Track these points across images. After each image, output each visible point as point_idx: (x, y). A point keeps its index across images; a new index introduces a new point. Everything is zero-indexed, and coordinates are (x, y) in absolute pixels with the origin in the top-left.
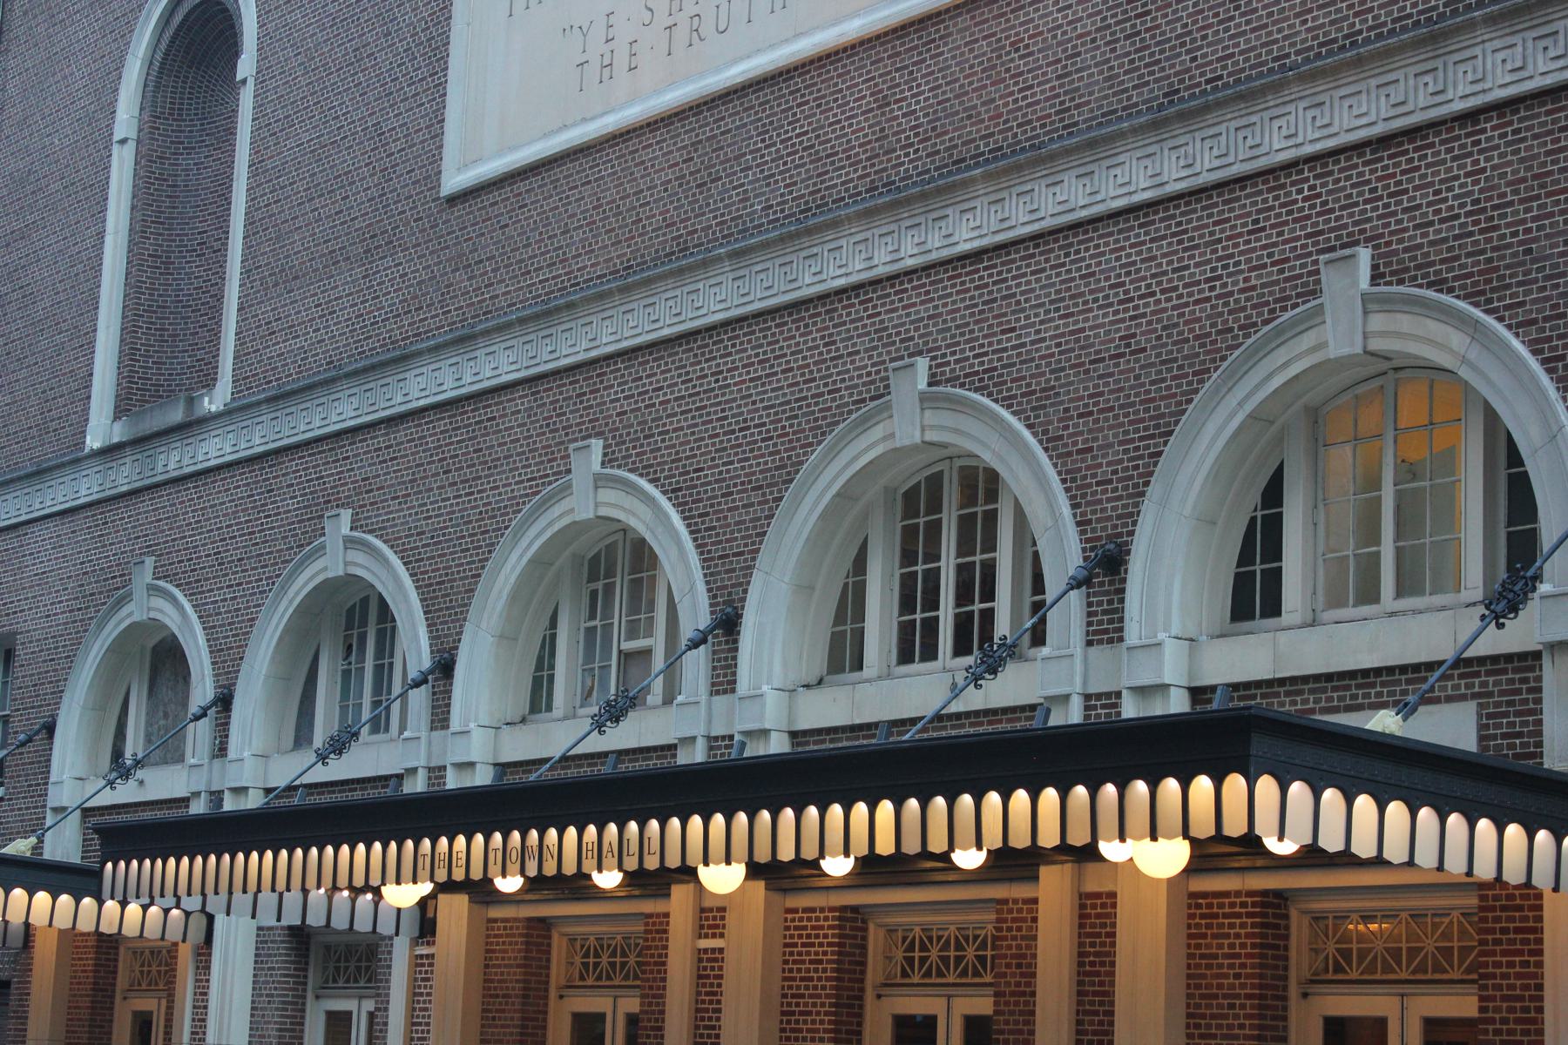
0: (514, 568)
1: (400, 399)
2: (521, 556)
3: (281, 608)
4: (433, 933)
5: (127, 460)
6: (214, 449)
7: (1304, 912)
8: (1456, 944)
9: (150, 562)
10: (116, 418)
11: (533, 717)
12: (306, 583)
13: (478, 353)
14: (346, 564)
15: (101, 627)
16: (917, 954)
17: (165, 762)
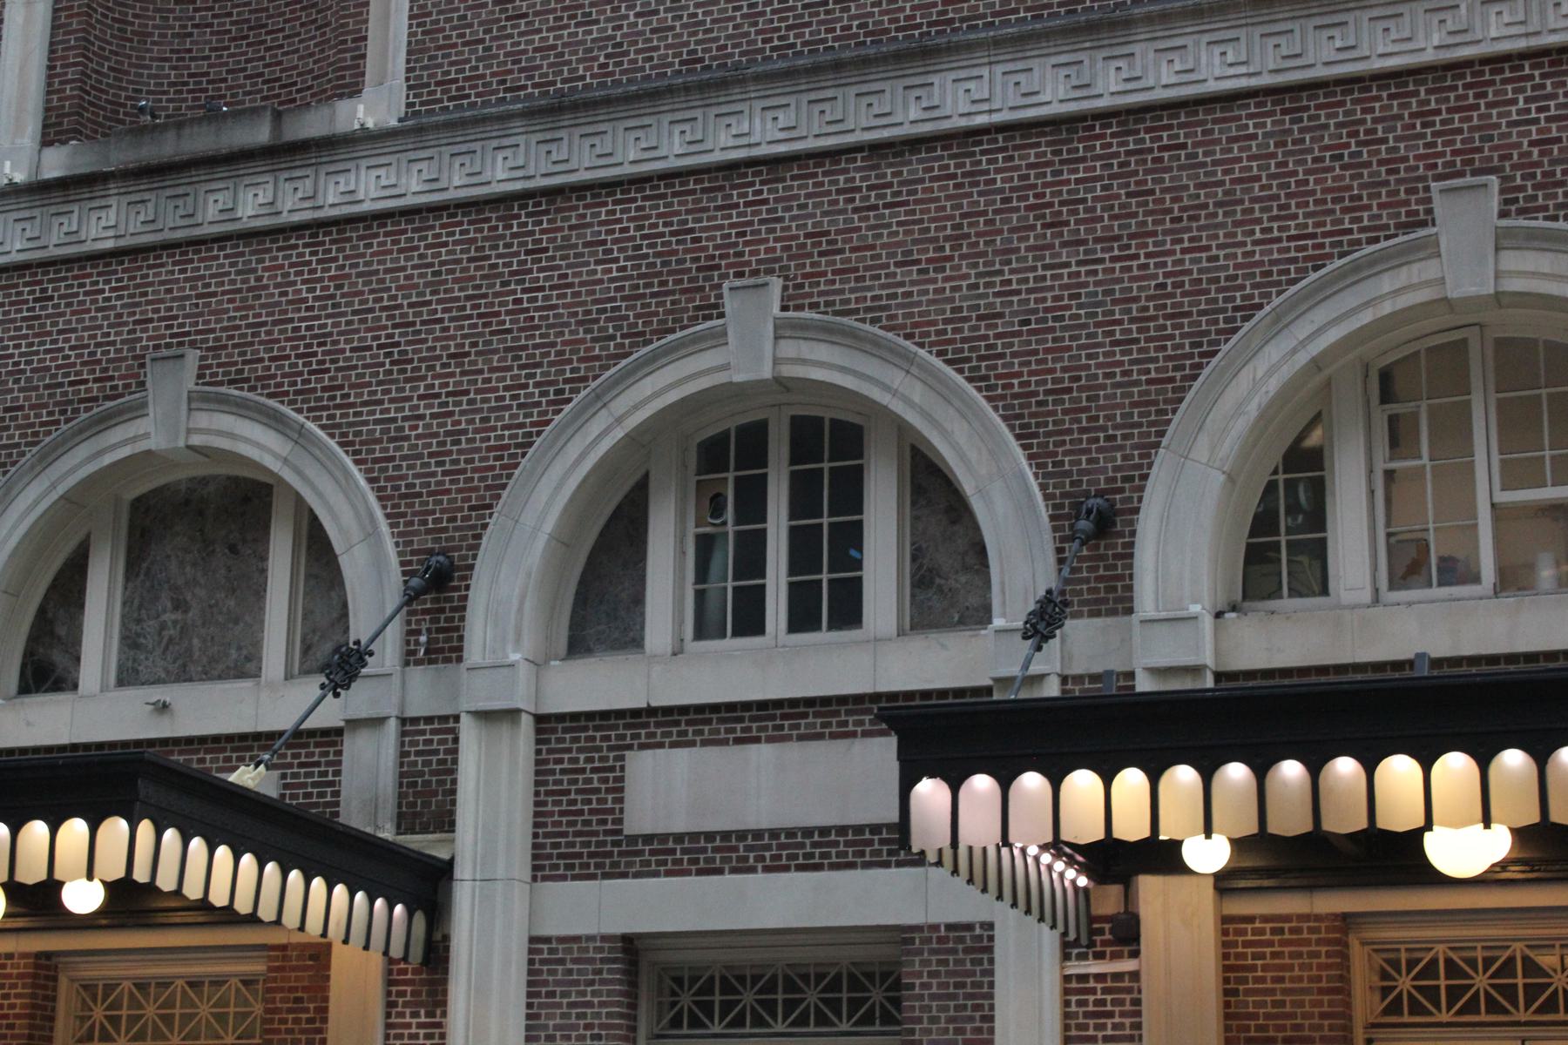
0: (1270, 372)
1: (914, 113)
2: (1294, 351)
3: (595, 427)
4: (1136, 939)
5: (113, 201)
6: (369, 186)
7: (72, 980)
8: (232, 1010)
9: (193, 357)
10: (46, 142)
11: (1246, 604)
12: (657, 395)
13: (1136, 48)
14: (776, 361)
15: (46, 459)
16: (124, 1012)
17: (1095, 610)
